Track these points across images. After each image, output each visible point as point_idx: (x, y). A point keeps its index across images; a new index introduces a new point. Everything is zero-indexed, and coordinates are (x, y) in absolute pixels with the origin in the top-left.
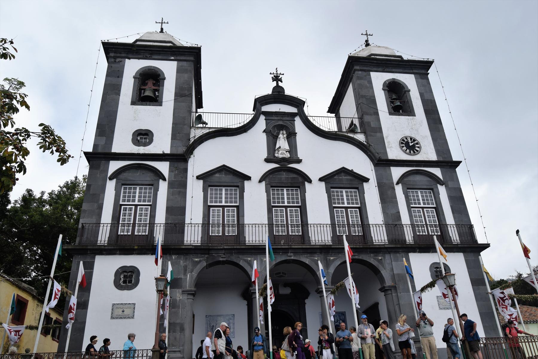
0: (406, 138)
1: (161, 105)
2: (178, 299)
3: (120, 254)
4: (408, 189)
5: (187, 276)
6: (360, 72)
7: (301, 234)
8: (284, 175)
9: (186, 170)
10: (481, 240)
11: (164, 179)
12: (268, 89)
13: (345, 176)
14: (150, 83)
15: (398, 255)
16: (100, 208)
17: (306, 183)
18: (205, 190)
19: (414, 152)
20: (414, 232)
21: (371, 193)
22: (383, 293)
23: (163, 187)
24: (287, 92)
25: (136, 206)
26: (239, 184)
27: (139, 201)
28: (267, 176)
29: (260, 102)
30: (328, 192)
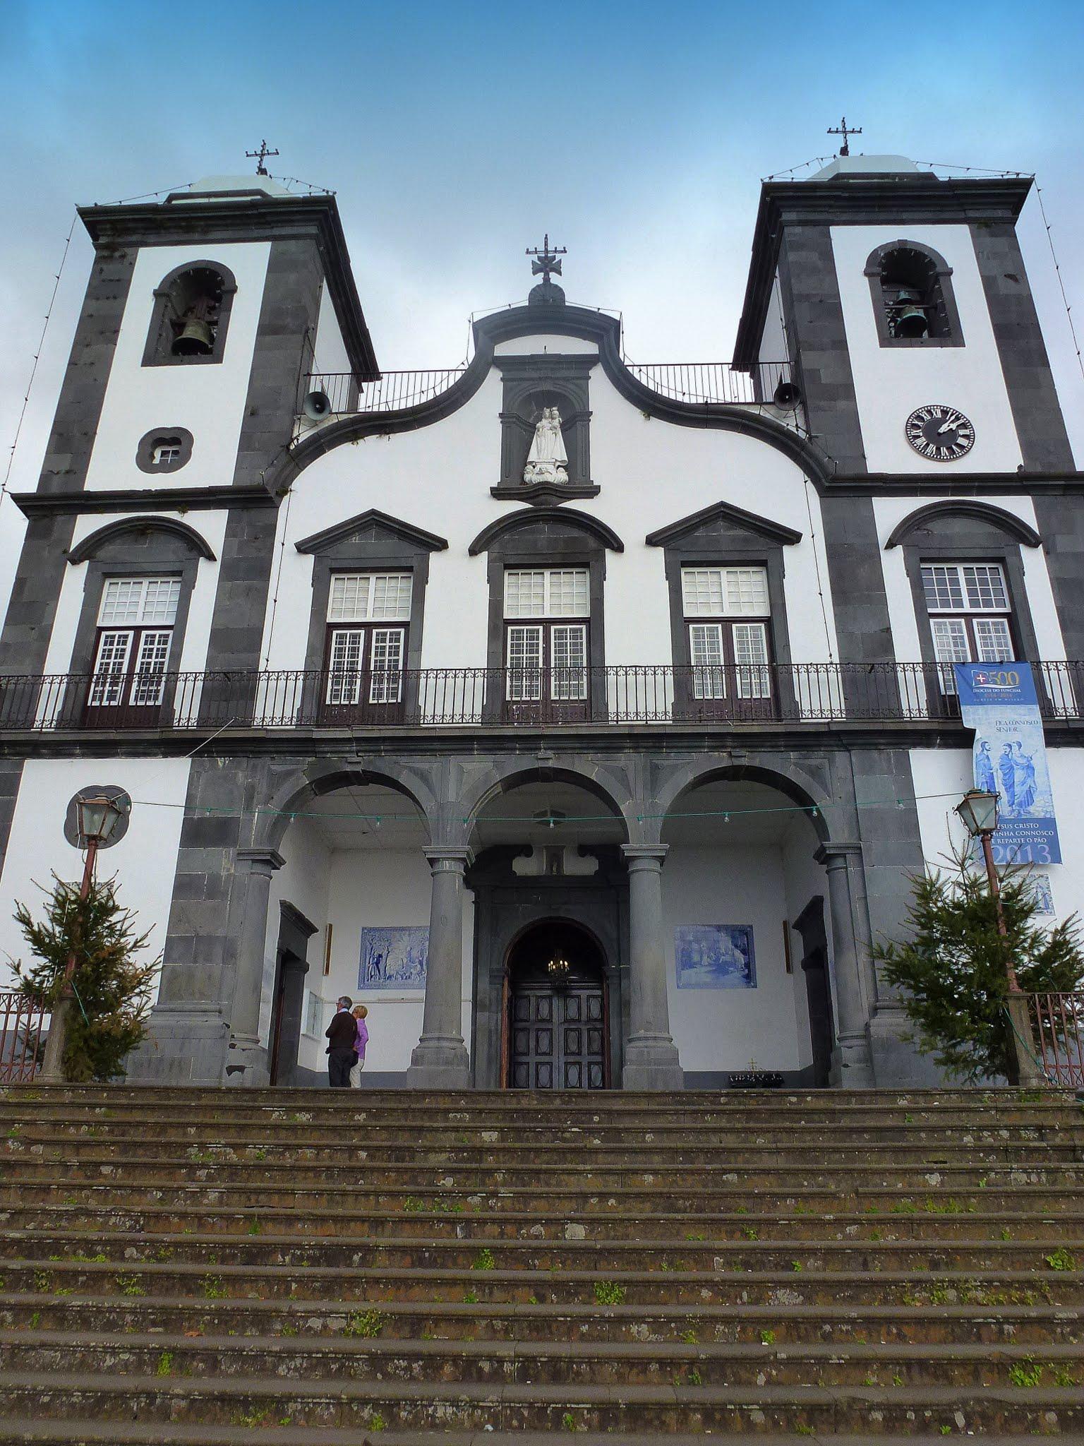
1: (219, 360)
2: (224, 873)
3: (84, 755)
4: (923, 560)
5: (252, 813)
6: (798, 230)
7: (585, 697)
8: (545, 534)
9: (271, 530)
11: (211, 558)
12: (514, 292)
13: (729, 529)
15: (875, 754)
16: (45, 637)
19: (950, 449)
20: (931, 684)
22: (825, 867)
23: (208, 576)
24: (574, 299)
26: (414, 563)
28: (494, 537)
29: (492, 330)
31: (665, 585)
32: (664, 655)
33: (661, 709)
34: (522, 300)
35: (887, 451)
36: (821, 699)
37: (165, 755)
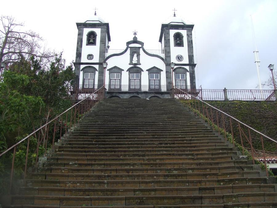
4: (176, 73)
8: (135, 69)
11: (97, 71)
14: (92, 36)
18: (110, 74)
21: (163, 75)
23: (97, 73)
24: (138, 40)
29: (128, 43)
30: (149, 75)
32: (147, 84)
34: (132, 40)
35: (174, 60)
36: (164, 89)
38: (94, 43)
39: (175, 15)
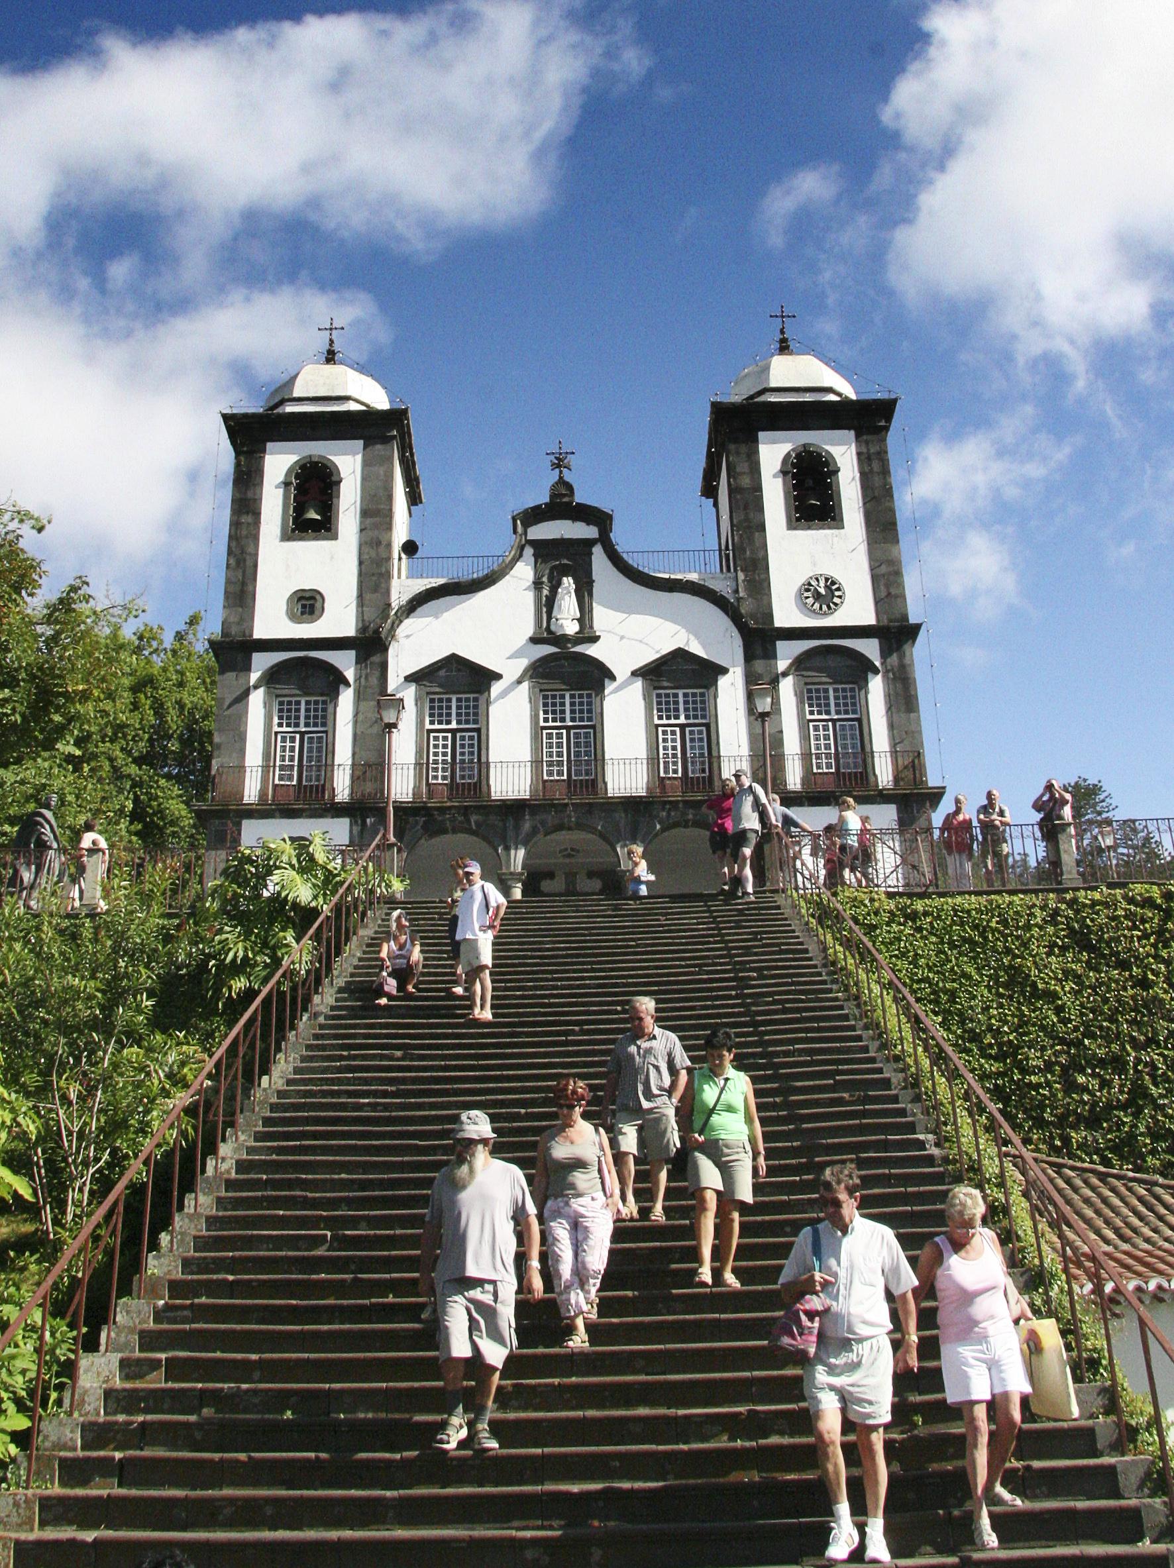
0: (817, 579)
1: (335, 537)
10: (933, 780)
11: (348, 684)
16: (241, 738)
17: (607, 681)
19: (829, 607)
24: (581, 497)
25: (302, 734)
27: (307, 725)
31: (642, 703)
33: (640, 786)
34: (543, 498)
37: (332, 817)
38: (324, 527)
39: (783, 341)
